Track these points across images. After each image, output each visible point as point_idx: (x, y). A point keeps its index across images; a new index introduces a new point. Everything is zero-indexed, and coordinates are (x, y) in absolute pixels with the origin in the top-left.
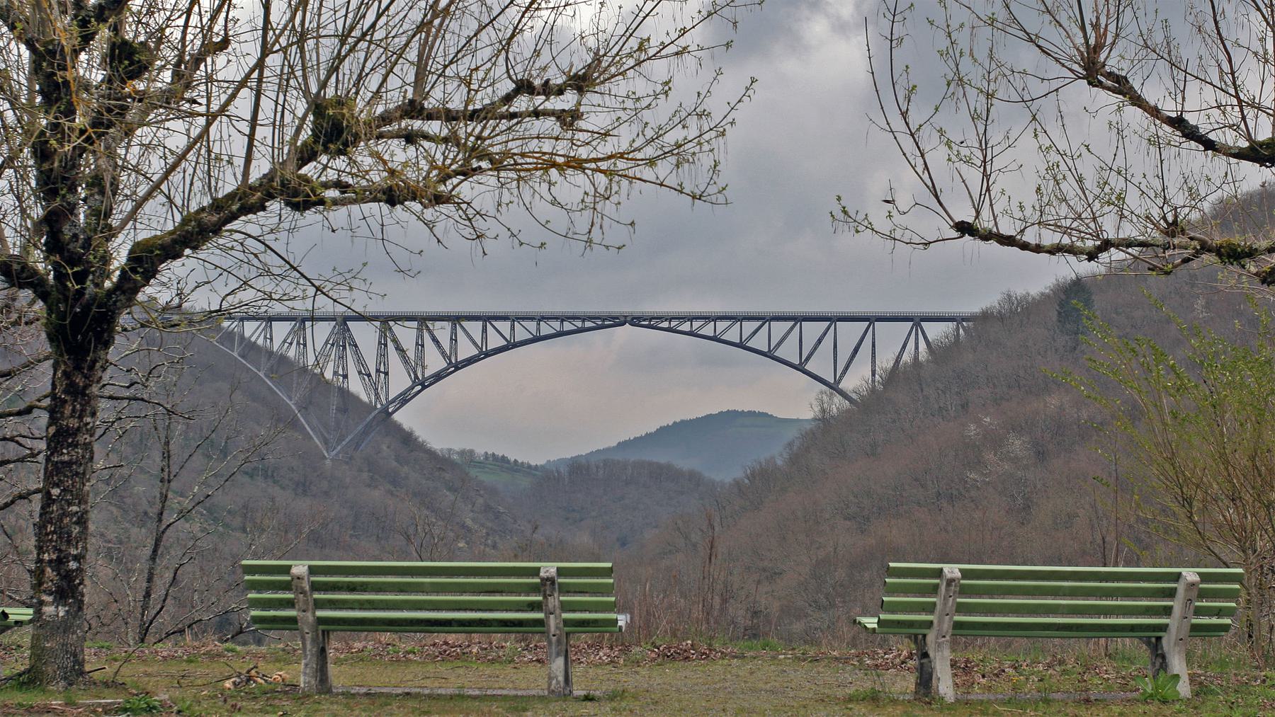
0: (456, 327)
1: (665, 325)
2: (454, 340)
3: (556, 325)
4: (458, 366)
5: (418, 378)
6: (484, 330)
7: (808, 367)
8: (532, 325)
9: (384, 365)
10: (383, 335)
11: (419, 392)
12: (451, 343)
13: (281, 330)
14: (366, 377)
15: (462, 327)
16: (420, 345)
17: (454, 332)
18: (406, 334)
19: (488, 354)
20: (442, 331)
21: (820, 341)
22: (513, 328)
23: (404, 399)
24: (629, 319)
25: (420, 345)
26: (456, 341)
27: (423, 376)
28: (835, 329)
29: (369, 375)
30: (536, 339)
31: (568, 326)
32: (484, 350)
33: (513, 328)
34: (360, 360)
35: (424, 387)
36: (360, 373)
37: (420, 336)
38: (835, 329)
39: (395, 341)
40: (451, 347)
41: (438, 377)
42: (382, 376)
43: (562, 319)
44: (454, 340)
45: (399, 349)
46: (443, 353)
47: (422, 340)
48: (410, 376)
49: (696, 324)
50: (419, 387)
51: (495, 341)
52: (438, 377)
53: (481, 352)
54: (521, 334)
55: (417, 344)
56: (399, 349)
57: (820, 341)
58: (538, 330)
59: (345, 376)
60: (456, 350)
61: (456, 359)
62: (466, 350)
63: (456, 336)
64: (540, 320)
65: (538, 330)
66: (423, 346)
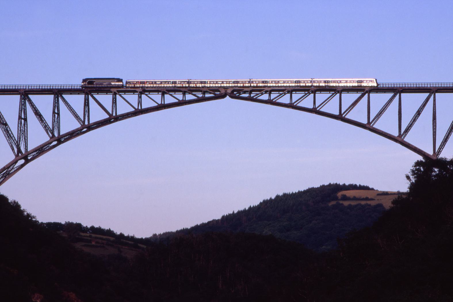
0: (58, 100)
1: (265, 97)
2: (56, 113)
3: (157, 98)
4: (61, 140)
5: (21, 152)
6: (87, 104)
7: (407, 139)
8: (133, 98)
11: (22, 166)
12: (54, 116)
15: (64, 100)
16: (23, 119)
17: (56, 105)
19: (90, 128)
21: (419, 113)
22: (114, 102)
24: (229, 91)
25: (23, 119)
26: (58, 114)
27: (26, 149)
28: (434, 100)
30: (138, 112)
31: (169, 99)
32: (86, 123)
33: (114, 102)
35: (27, 161)
37: (22, 109)
38: (434, 100)
40: (53, 121)
41: (41, 150)
43: (164, 91)
44: (56, 113)
46: (46, 127)
47: (25, 114)
48: (13, 149)
49: (296, 96)
50: (22, 162)
52: (41, 150)
53: (83, 126)
54: (123, 108)
55: (20, 118)
57: (419, 113)
58: (140, 102)
60: (59, 122)
61: (59, 133)
63: (58, 110)
64: (141, 93)
65: (140, 102)
66: (25, 120)
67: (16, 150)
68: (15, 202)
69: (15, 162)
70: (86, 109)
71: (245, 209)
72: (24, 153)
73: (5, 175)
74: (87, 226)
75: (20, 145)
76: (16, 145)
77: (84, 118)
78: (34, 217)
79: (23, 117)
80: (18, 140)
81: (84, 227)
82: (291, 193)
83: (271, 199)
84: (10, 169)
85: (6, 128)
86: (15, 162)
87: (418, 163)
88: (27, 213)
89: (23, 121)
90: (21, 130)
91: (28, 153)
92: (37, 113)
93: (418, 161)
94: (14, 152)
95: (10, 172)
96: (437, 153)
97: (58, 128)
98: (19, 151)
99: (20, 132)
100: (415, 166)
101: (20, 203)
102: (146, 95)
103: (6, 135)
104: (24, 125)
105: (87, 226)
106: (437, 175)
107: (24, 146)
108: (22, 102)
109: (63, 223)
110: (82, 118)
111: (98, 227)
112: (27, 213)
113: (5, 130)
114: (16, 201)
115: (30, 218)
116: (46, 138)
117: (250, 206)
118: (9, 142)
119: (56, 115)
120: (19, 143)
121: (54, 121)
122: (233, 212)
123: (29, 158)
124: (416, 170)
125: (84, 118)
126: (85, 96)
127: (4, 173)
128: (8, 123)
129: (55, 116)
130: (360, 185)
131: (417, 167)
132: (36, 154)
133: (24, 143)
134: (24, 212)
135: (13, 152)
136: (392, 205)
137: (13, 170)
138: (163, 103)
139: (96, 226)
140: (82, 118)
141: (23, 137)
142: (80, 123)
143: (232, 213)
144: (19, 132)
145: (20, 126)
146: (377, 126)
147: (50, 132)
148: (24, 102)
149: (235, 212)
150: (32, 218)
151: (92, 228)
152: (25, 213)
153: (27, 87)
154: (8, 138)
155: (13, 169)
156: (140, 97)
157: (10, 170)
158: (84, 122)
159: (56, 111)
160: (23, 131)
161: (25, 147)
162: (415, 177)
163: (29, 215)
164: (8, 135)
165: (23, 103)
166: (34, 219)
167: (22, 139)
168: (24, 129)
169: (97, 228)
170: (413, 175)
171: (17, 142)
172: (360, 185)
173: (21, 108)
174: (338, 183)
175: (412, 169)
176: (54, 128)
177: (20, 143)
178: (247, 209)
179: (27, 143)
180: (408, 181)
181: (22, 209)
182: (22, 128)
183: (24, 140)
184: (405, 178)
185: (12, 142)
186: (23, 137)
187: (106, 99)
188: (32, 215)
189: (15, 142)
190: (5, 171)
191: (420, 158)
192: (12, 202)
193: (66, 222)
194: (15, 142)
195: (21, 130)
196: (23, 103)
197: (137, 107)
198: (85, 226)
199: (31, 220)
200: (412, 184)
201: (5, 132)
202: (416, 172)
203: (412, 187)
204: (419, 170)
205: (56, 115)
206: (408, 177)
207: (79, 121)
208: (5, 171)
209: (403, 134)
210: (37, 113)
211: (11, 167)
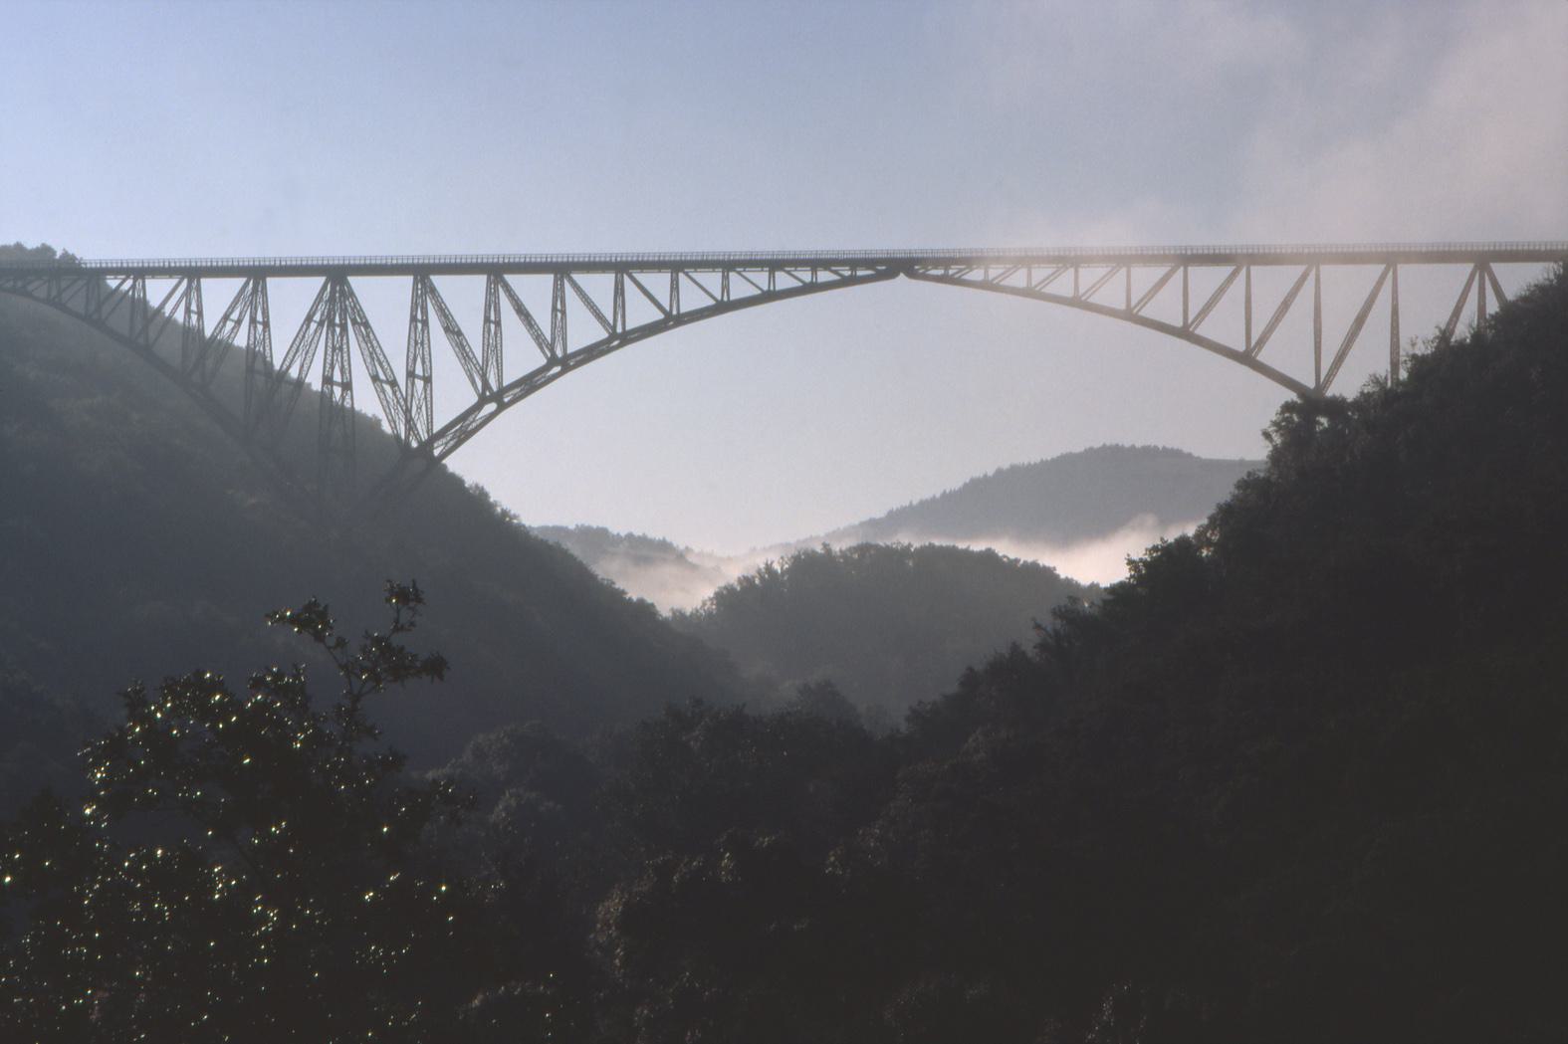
0: (562, 285)
2: (559, 310)
3: (761, 278)
5: (490, 389)
7: (1263, 357)
9: (423, 363)
10: (418, 303)
13: (218, 295)
14: (387, 388)
17: (558, 295)
18: (464, 296)
20: (535, 290)
23: (463, 429)
25: (492, 321)
28: (1318, 280)
29: (394, 384)
32: (619, 330)
34: (374, 354)
35: (502, 407)
36: (375, 378)
37: (491, 303)
38: (1318, 280)
39: (444, 313)
42: (419, 384)
44: (559, 310)
45: (453, 331)
46: (538, 338)
47: (498, 312)
48: (473, 383)
51: (640, 313)
54: (692, 299)
56: (453, 331)
58: (725, 288)
59: (347, 386)
60: (564, 328)
62: (583, 331)
65: (725, 288)
68: (477, 486)
69: (477, 407)
70: (619, 302)
71: (934, 497)
73: (458, 434)
74: (618, 534)
77: (615, 320)
78: (515, 517)
79: (493, 318)
81: (613, 536)
82: (1026, 463)
83: (985, 476)
84: (467, 422)
86: (477, 407)
87: (1288, 407)
88: (502, 509)
89: (493, 326)
91: (503, 391)
93: (1287, 403)
94: (476, 388)
96: (1321, 387)
98: (486, 385)
100: (1282, 412)
101: (487, 489)
102: (739, 273)
103: (460, 355)
104: (496, 334)
105: (618, 534)
106: (1326, 431)
109: (572, 527)
110: (610, 318)
111: (641, 534)
112: (502, 509)
113: (457, 344)
114: (480, 485)
115: (507, 519)
117: (945, 492)
119: (559, 315)
122: (911, 503)
123: (506, 400)
124: (1285, 419)
125: (615, 320)
126: (616, 277)
127: (457, 431)
128: (463, 330)
129: (556, 315)
130: (1164, 448)
131: (1287, 415)
134: (496, 505)
136: (1236, 492)
137: (474, 425)
138: (772, 288)
139: (638, 533)
140: (610, 318)
142: (607, 330)
143: (908, 504)
144: (486, 349)
145: (486, 335)
146: (1203, 330)
149: (915, 503)
150: (511, 518)
151: (630, 536)
152: (499, 510)
154: (463, 361)
155: (474, 421)
156: (725, 278)
157: (469, 425)
158: (614, 327)
159: (559, 307)
160: (494, 346)
162: (1282, 435)
163: (505, 513)
166: (515, 521)
167: (492, 362)
169: (639, 537)
170: (1277, 431)
172: (1164, 448)
174: (1120, 444)
175: (1274, 419)
178: (938, 495)
180: (1267, 443)
181: (492, 500)
184: (1262, 438)
188: (512, 512)
190: (458, 427)
191: (1292, 396)
192: (471, 488)
193: (577, 526)
195: (488, 345)
197: (719, 298)
198: (615, 533)
199: (510, 523)
200: (1275, 448)
201: (457, 349)
202: (1283, 424)
203: (1276, 457)
204: (1289, 420)
205: (559, 315)
206: (1267, 435)
207: (604, 326)
208: (458, 427)
209: (1255, 347)
211: (471, 419)
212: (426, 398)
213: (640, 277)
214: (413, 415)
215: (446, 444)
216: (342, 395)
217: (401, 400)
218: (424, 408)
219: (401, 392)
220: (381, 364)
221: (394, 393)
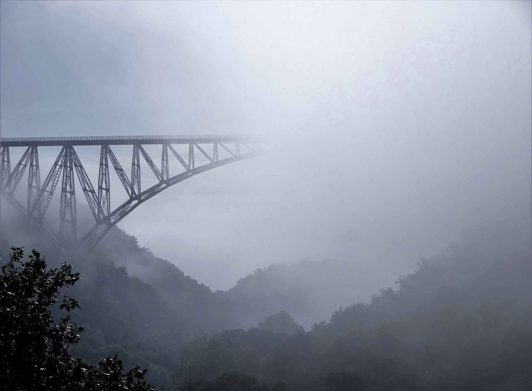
0: (167, 149)
5: (135, 194)
9: (106, 183)
14: (90, 194)
15: (172, 149)
29: (93, 192)
32: (191, 168)
35: (140, 202)
36: (85, 190)
37: (136, 156)
39: (114, 161)
42: (104, 192)
45: (119, 170)
46: (156, 172)
48: (128, 191)
56: (119, 170)
59: (73, 193)
67: (130, 192)
69: (129, 202)
70: (191, 156)
72: (137, 194)
73: (121, 213)
75: (134, 188)
76: (130, 188)
77: (189, 164)
79: (136, 163)
80: (132, 183)
84: (125, 208)
85: (121, 173)
89: (136, 167)
90: (134, 174)
91: (141, 194)
92: (149, 161)
94: (129, 194)
95: (125, 211)
97: (167, 172)
99: (134, 177)
103: (122, 179)
104: (137, 170)
107: (138, 188)
108: (135, 150)
110: (188, 164)
116: (157, 182)
118: (124, 185)
119: (165, 162)
120: (133, 186)
121: (164, 167)
123: (142, 199)
125: (189, 164)
126: (190, 145)
127: (120, 212)
129: (164, 162)
132: (148, 195)
133: (138, 186)
135: (128, 194)
137: (128, 209)
140: (188, 164)
141: (136, 181)
142: (186, 168)
144: (133, 176)
145: (133, 171)
147: (160, 176)
148: (137, 150)
153: (140, 138)
155: (128, 208)
157: (126, 209)
158: (189, 167)
161: (138, 189)
164: (123, 179)
165: (136, 151)
168: (137, 174)
171: (131, 185)
173: (135, 156)
176: (163, 173)
177: (134, 186)
179: (140, 185)
182: (135, 173)
183: (137, 183)
185: (127, 185)
186: (136, 181)
187: (208, 147)
189: (130, 185)
190: (121, 210)
194: (130, 185)
195: (134, 174)
196: (136, 151)
197: (235, 154)
205: (165, 162)
208: (121, 210)
210: (149, 161)
211: (127, 207)
212: (107, 198)
213: (200, 145)
214: (101, 205)
215: (116, 218)
216: (70, 197)
217: (96, 199)
218: (106, 202)
219: (96, 195)
220: (87, 184)
221: (93, 196)
